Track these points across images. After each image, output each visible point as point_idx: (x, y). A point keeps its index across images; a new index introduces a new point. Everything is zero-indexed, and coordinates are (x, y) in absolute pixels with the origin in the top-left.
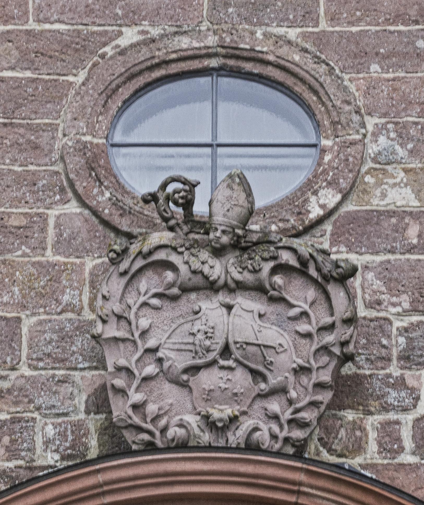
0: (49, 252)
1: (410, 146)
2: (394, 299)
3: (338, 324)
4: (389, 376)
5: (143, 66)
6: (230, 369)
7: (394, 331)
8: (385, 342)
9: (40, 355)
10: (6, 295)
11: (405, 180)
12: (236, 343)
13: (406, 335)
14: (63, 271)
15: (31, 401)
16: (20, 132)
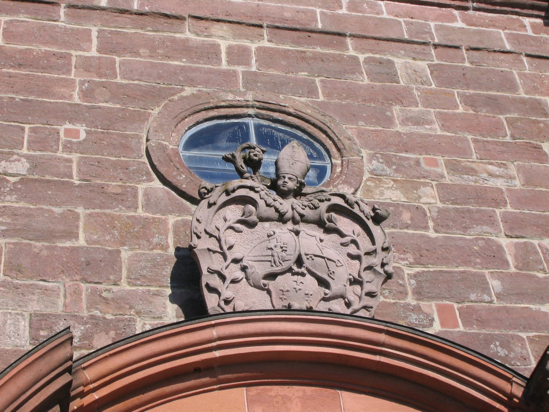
0: (140, 210)
1: (394, 167)
2: (402, 256)
3: (379, 250)
4: (409, 305)
5: (202, 107)
6: (303, 275)
7: (406, 276)
8: (401, 282)
9: (137, 276)
10: (107, 235)
11: (395, 186)
12: (306, 255)
13: (415, 278)
14: (152, 223)
15: (131, 308)
16: (113, 137)
